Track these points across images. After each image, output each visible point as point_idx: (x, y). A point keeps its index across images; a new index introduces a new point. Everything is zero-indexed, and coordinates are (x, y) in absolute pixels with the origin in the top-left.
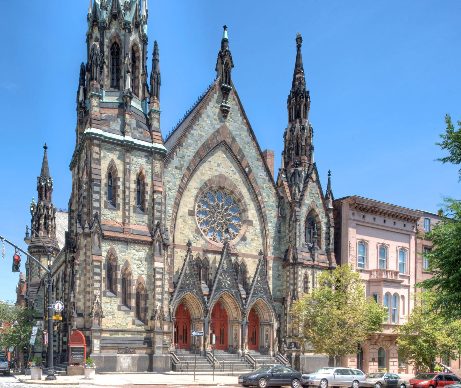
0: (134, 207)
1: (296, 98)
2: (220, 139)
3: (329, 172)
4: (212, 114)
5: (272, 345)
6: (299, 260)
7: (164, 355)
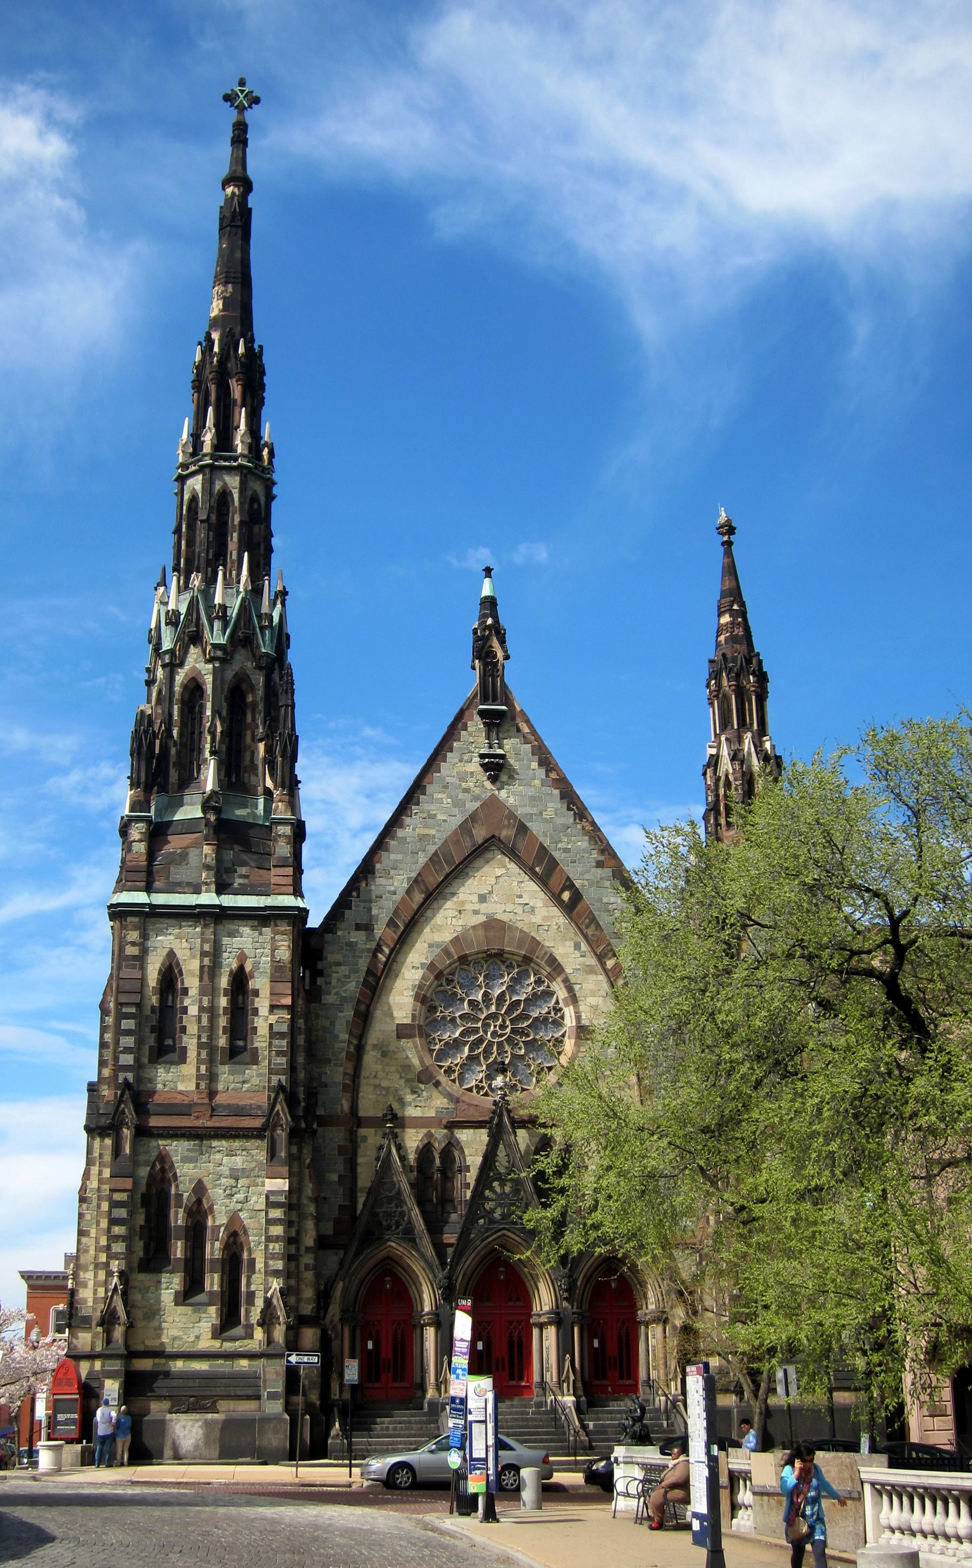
2: (480, 834)
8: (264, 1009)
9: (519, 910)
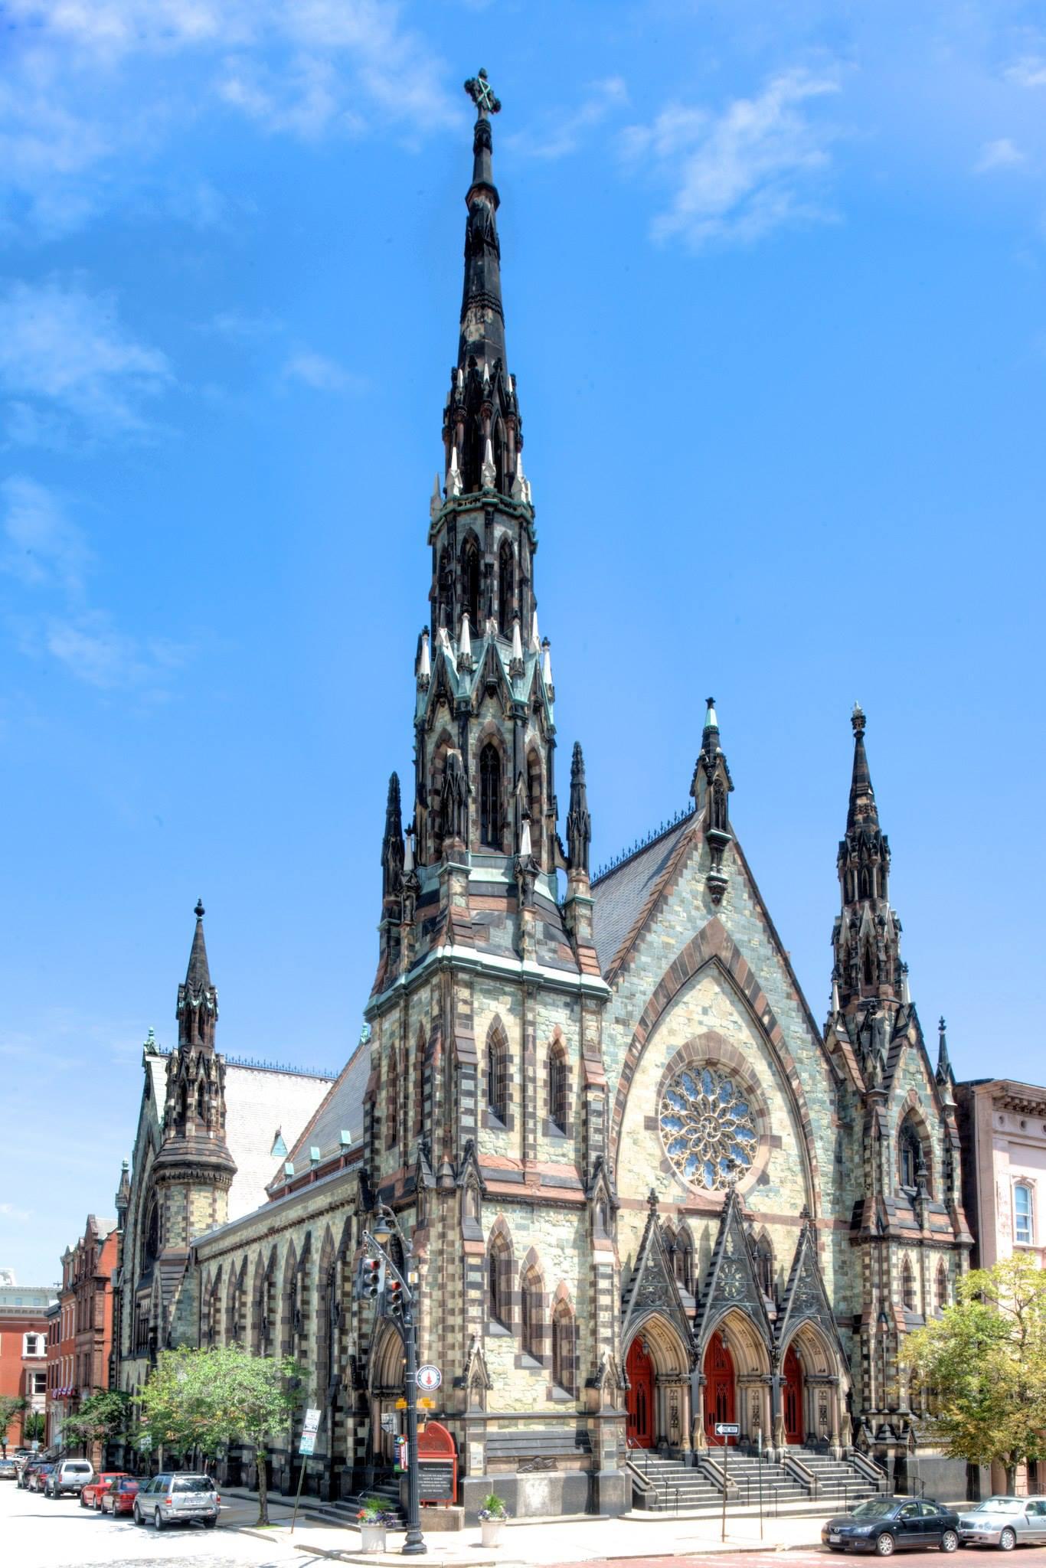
0: (545, 1122)
1: (860, 851)
2: (707, 951)
3: (942, 1022)
4: (689, 896)
5: (836, 1432)
6: (892, 1231)
7: (622, 1474)
9: (731, 1026)
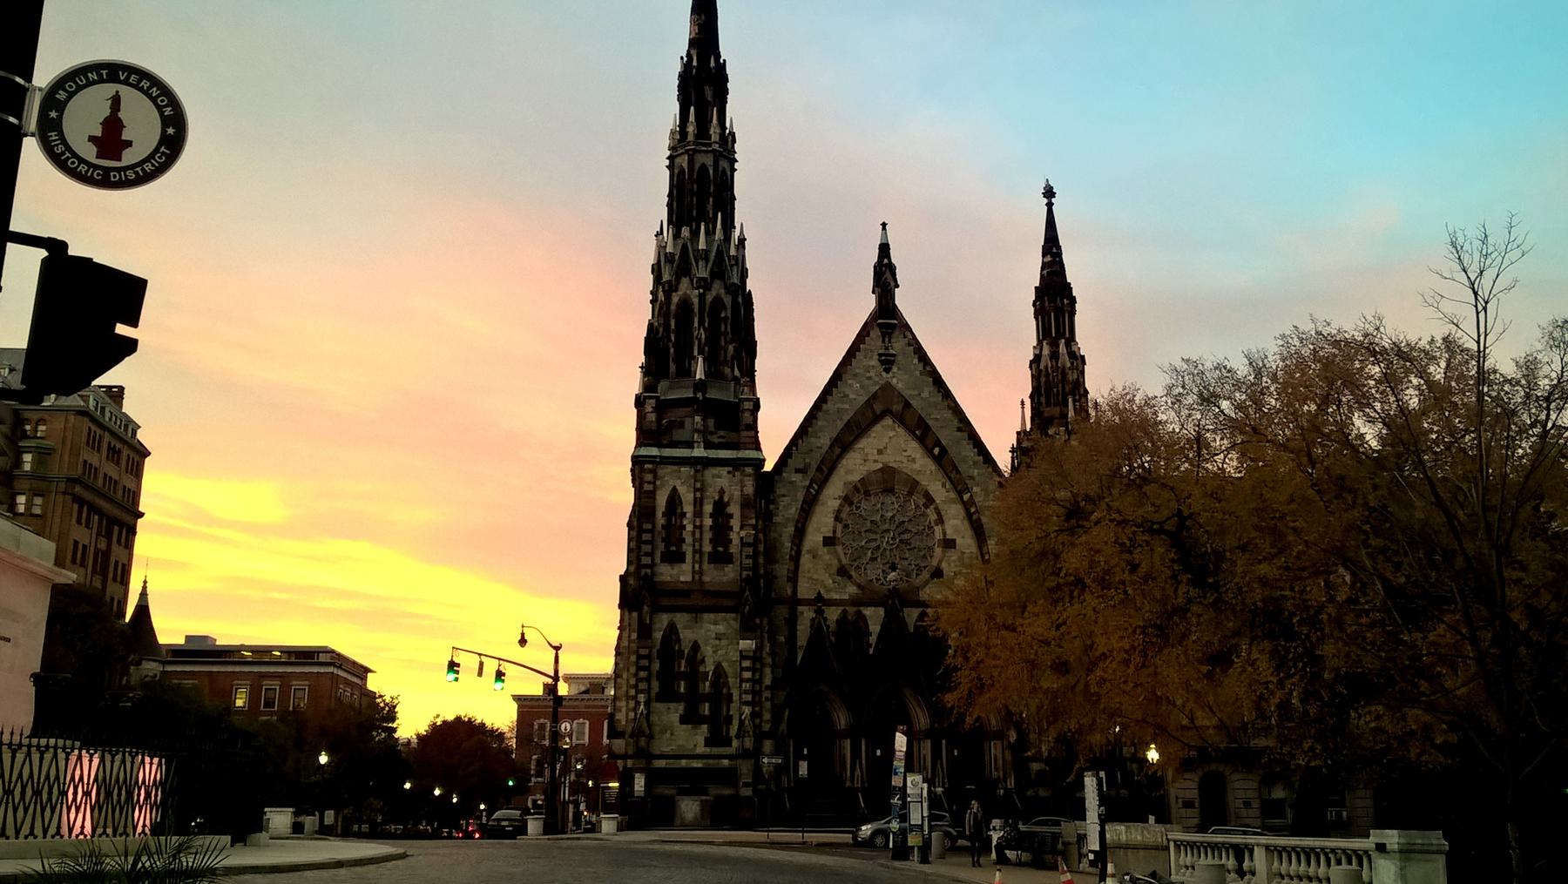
2: (878, 408)
8: (736, 528)
